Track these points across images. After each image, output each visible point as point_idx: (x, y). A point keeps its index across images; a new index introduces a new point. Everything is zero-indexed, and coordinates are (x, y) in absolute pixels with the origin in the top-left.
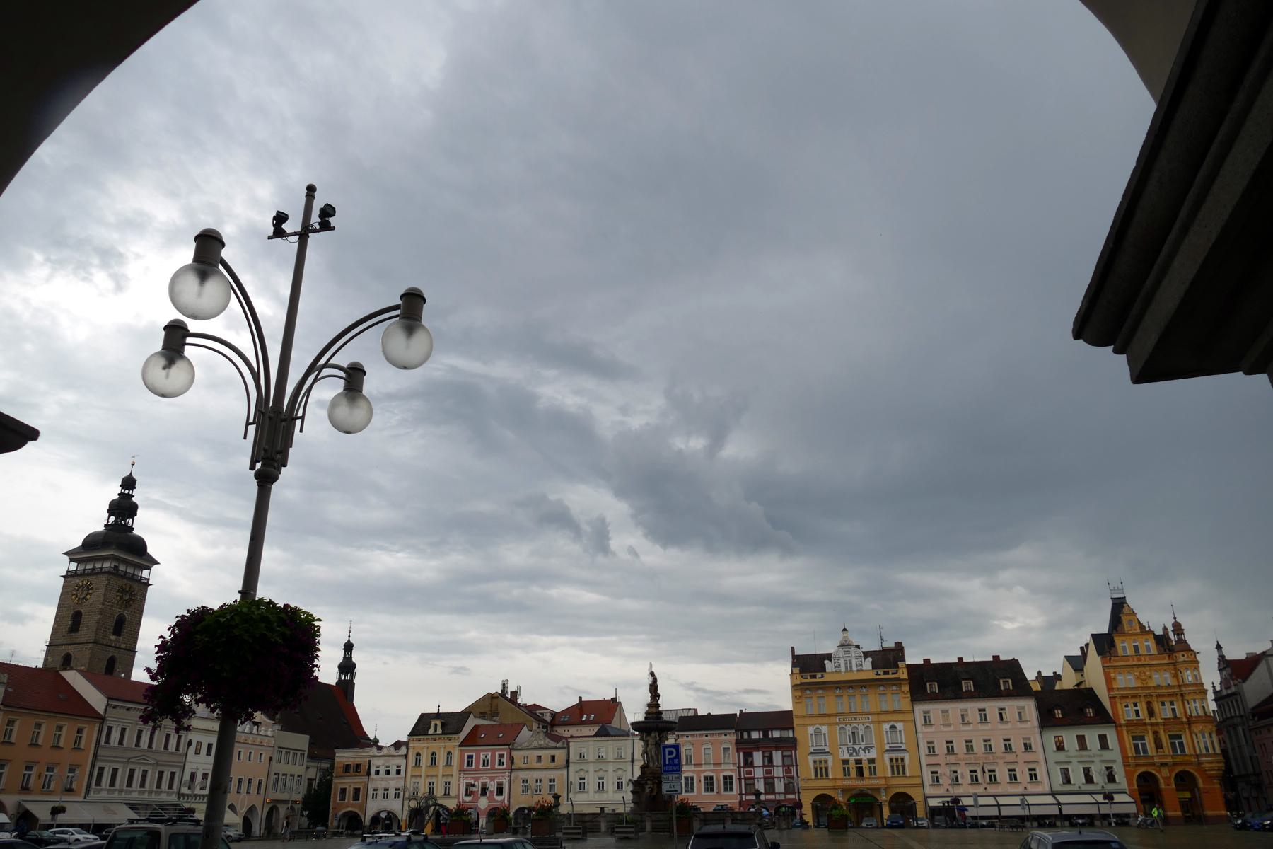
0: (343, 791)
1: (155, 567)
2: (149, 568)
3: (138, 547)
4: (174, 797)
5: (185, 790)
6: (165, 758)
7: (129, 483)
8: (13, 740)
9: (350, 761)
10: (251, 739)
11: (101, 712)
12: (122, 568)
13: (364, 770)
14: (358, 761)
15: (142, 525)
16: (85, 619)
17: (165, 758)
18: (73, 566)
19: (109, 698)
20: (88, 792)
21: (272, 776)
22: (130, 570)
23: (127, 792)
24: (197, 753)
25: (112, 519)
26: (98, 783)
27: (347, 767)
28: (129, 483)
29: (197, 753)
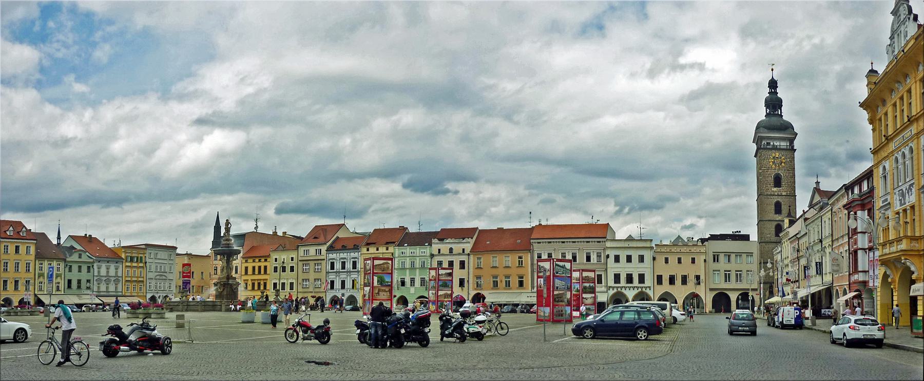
24: (617, 259)
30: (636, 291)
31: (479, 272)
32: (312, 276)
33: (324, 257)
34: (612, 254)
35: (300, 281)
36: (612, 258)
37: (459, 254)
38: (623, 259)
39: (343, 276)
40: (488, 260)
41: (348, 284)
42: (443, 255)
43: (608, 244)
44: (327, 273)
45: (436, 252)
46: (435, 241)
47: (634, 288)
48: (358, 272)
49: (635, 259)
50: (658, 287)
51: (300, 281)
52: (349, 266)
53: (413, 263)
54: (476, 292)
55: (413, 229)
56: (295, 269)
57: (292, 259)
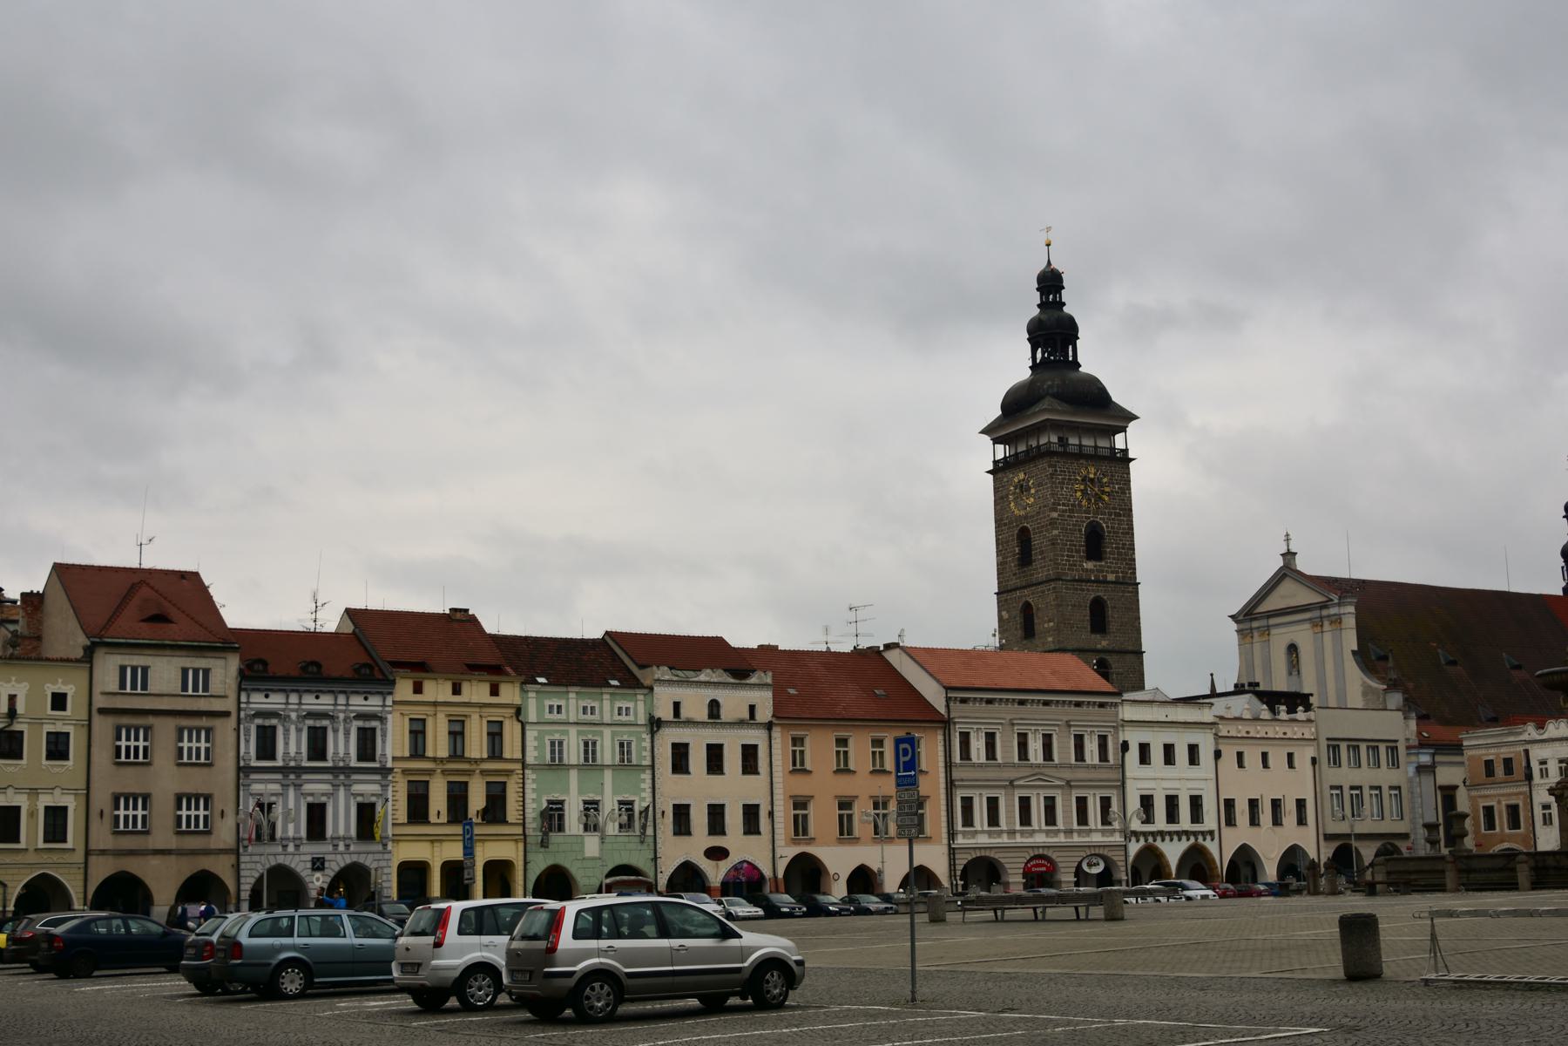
0: (1489, 811)
1: (1132, 426)
2: (1123, 429)
3: (1094, 398)
4: (1118, 838)
5: (1136, 825)
6: (1081, 774)
7: (1050, 283)
8: (808, 766)
9: (1491, 754)
10: (1259, 730)
11: (943, 710)
12: (1073, 441)
13: (1519, 768)
14: (1505, 752)
15: (1092, 358)
16: (1037, 541)
17: (1081, 774)
18: (1001, 451)
19: (947, 689)
20: (952, 835)
21: (1327, 792)
22: (1088, 442)
23: (1022, 833)
24: (1144, 757)
25: (1039, 355)
26: (968, 820)
27: (1489, 765)
28: (1050, 283)
29: (1144, 757)
30: (1184, 845)
31: (802, 786)
32: (165, 779)
33: (229, 705)
34: (1134, 738)
35: (101, 799)
36: (1133, 755)
37: (740, 723)
38: (1157, 754)
39: (317, 787)
40: (820, 747)
41: (341, 820)
42: (690, 723)
43: (1128, 712)
44: (243, 771)
45: (665, 713)
46: (663, 673)
47: (1179, 834)
48: (385, 771)
49: (1181, 754)
50: (1226, 831)
51: (101, 799)
52: (342, 746)
53: (589, 748)
54: (793, 851)
55: (497, 621)
56: (75, 746)
57: (59, 701)
